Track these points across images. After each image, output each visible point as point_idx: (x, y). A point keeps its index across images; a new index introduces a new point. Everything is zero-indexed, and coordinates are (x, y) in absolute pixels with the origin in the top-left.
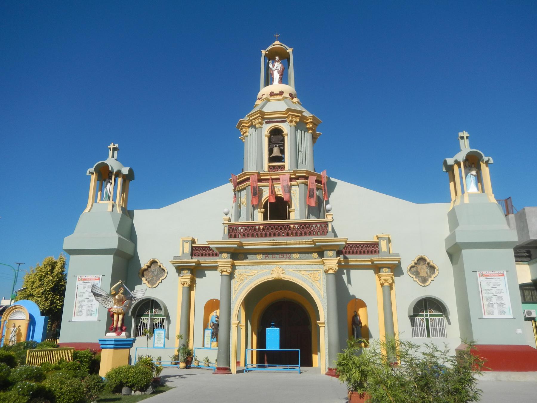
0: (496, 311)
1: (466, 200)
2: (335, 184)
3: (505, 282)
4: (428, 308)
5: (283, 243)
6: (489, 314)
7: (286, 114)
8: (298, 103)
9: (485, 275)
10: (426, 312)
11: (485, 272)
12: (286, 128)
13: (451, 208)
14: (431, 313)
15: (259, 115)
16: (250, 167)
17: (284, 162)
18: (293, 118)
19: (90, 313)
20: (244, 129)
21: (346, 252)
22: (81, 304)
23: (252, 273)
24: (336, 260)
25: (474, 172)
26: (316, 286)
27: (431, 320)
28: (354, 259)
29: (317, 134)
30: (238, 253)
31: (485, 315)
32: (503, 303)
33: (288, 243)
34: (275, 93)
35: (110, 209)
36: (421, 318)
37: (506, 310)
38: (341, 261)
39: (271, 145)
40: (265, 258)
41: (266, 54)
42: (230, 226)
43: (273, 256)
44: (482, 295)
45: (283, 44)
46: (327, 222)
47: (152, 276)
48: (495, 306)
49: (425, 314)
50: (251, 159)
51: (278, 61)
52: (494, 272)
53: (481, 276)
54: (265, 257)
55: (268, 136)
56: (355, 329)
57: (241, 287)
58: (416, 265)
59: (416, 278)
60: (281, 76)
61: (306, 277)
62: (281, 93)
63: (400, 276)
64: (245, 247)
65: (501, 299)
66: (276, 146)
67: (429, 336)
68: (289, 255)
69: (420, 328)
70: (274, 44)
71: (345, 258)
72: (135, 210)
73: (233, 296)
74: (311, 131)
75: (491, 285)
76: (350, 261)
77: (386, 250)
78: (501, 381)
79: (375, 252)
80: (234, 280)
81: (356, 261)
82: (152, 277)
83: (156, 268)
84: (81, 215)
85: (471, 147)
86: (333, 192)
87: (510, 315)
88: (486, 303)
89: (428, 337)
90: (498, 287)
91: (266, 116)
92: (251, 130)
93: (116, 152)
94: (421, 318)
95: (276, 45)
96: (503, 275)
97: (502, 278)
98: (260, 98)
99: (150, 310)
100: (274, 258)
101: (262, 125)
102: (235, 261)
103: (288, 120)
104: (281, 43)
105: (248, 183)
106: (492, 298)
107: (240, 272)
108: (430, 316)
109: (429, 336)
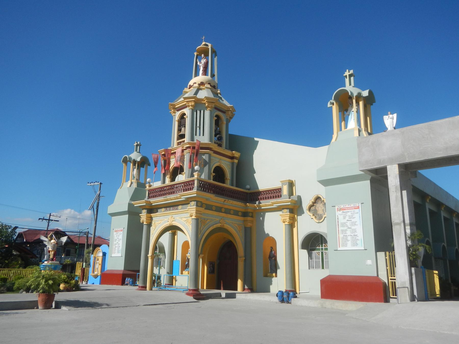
0: (349, 243)
2: (258, 142)
3: (360, 215)
4: (323, 243)
5: (169, 199)
6: (343, 246)
9: (343, 209)
10: (322, 246)
11: (342, 207)
14: (326, 247)
19: (118, 252)
26: (189, 228)
27: (325, 253)
28: (263, 204)
29: (229, 107)
31: (339, 247)
32: (356, 235)
36: (317, 252)
37: (358, 242)
39: (181, 127)
42: (149, 191)
44: (338, 228)
45: (207, 43)
46: (194, 180)
48: (349, 238)
49: (321, 248)
52: (351, 205)
53: (339, 211)
55: (177, 121)
57: (154, 232)
58: (315, 204)
59: (314, 215)
60: (203, 69)
61: (184, 222)
63: (301, 215)
64: (153, 204)
65: (355, 231)
66: (183, 127)
67: (323, 268)
69: (315, 261)
70: (202, 45)
73: (151, 238)
74: (209, 109)
75: (347, 218)
76: (261, 206)
77: (286, 194)
78: (325, 308)
79: (278, 197)
81: (266, 205)
86: (256, 149)
87: (362, 246)
88: (341, 236)
89: (322, 269)
90: (353, 220)
91: (176, 107)
94: (317, 252)
96: (358, 208)
97: (357, 210)
101: (175, 114)
102: (151, 214)
104: (205, 43)
106: (347, 231)
108: (324, 250)
109: (323, 268)
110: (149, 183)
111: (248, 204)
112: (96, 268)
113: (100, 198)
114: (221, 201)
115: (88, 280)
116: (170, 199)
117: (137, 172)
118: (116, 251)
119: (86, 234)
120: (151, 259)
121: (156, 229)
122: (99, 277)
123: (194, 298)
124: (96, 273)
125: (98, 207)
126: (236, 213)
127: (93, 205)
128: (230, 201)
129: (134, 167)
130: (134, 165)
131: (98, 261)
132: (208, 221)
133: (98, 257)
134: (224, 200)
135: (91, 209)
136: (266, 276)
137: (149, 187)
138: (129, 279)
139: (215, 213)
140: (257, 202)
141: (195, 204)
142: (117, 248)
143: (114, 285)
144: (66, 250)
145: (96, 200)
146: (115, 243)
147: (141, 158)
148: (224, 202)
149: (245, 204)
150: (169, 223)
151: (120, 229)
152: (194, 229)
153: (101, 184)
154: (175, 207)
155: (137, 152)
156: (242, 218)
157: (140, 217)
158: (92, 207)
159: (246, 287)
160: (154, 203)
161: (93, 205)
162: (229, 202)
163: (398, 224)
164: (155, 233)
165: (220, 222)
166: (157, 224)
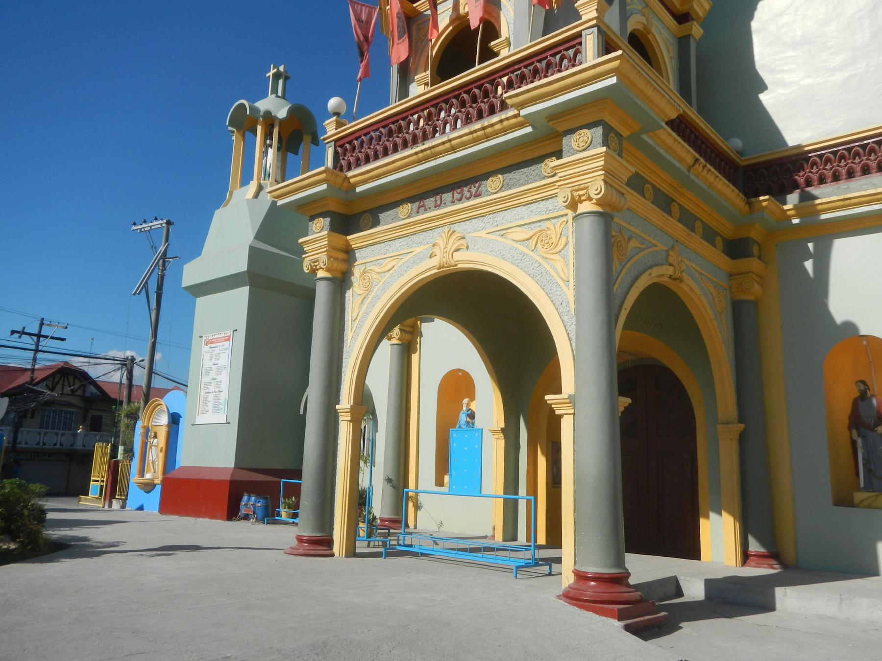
5: (441, 148)
19: (217, 410)
21: (809, 183)
22: (207, 391)
23: (388, 263)
24: (595, 157)
30: (359, 213)
33: (453, 142)
38: (789, 213)
40: (418, 212)
43: (436, 201)
46: (579, 35)
54: (419, 208)
56: (859, 441)
57: (363, 309)
64: (359, 189)
68: (477, 185)
71: (807, 198)
73: (348, 335)
76: (820, 207)
80: (351, 290)
100: (439, 206)
102: (349, 237)
107: (363, 267)
110: (337, 114)
111: (762, 198)
112: (150, 462)
113: (167, 264)
114: (681, 160)
115: (127, 496)
116: (448, 145)
117: (278, 161)
118: (210, 406)
119: (125, 365)
120: (350, 421)
121: (371, 297)
122: (158, 489)
123: (627, 628)
124: (148, 476)
125: (160, 287)
126: (710, 235)
127: (146, 283)
128: (709, 170)
129: (268, 142)
130: (268, 135)
131: (156, 440)
132: (633, 244)
133: (157, 429)
134: (694, 157)
135: (139, 294)
136: (843, 500)
137: (336, 129)
138: (253, 498)
139: (656, 215)
140: (793, 199)
141: (600, 140)
142: (211, 397)
143: (204, 517)
144: (90, 415)
145: (154, 269)
146: (205, 379)
147: (289, 108)
148: (689, 169)
149: (750, 204)
150: (435, 261)
151: (223, 335)
152: (592, 267)
153: (169, 223)
154: (465, 189)
155: (277, 96)
156: (725, 262)
157: (300, 251)
158: (144, 286)
159: (754, 546)
160: (365, 182)
161: (146, 283)
162: (705, 171)
164: (367, 314)
165: (671, 260)
166: (374, 276)
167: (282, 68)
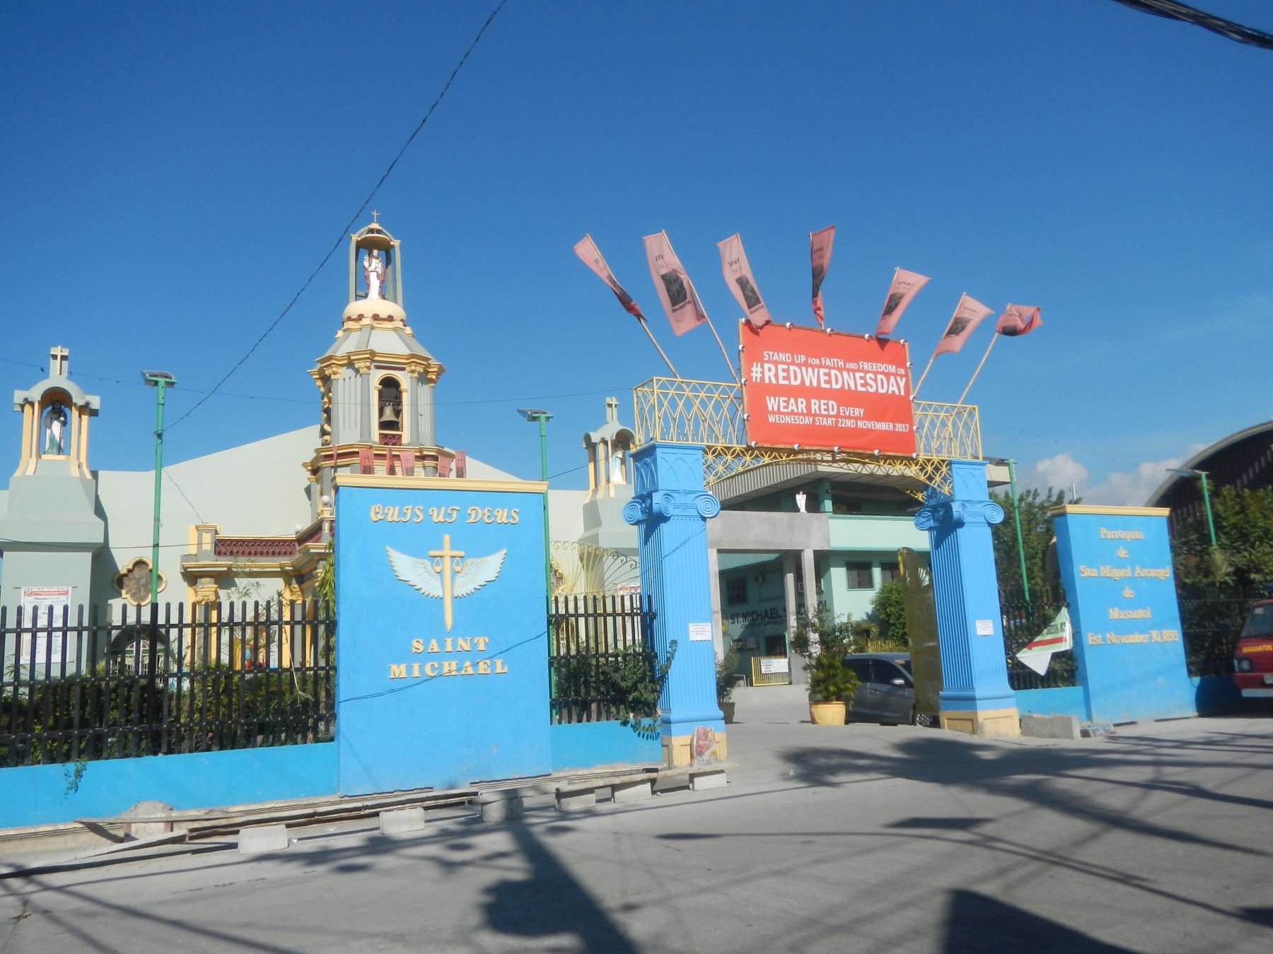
1: (612, 493)
7: (407, 359)
8: (413, 336)
12: (404, 379)
13: (587, 501)
15: (368, 356)
16: (344, 429)
17: (402, 431)
18: (416, 366)
20: (334, 369)
25: (620, 454)
34: (381, 316)
35: (75, 472)
41: (357, 241)
47: (136, 586)
50: (347, 418)
51: (377, 258)
62: (390, 319)
66: (390, 404)
72: (100, 472)
82: (137, 589)
83: (144, 572)
84: (11, 479)
85: (620, 420)
91: (376, 359)
92: (345, 373)
93: (65, 363)
95: (371, 231)
98: (352, 318)
99: (135, 643)
103: (408, 369)
105: (356, 460)
163: (717, 612)
167: (66, 353)
